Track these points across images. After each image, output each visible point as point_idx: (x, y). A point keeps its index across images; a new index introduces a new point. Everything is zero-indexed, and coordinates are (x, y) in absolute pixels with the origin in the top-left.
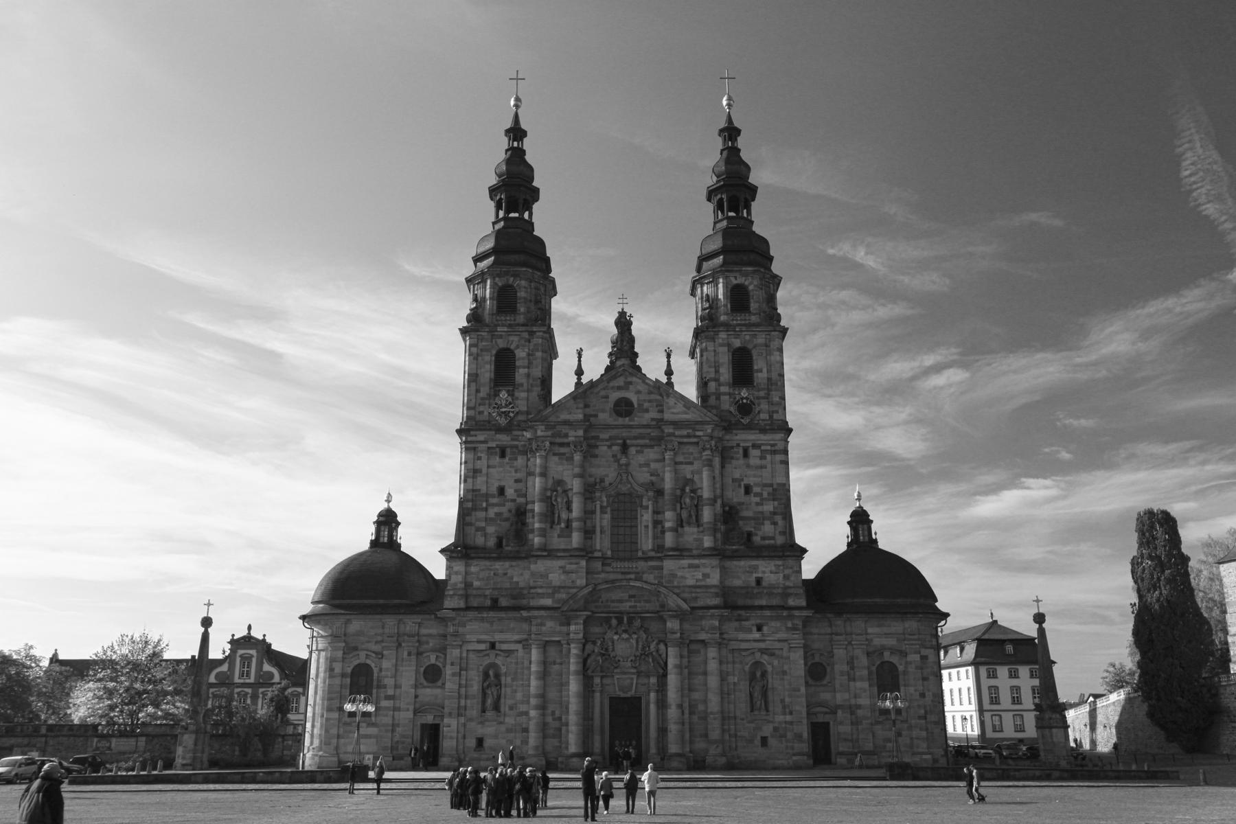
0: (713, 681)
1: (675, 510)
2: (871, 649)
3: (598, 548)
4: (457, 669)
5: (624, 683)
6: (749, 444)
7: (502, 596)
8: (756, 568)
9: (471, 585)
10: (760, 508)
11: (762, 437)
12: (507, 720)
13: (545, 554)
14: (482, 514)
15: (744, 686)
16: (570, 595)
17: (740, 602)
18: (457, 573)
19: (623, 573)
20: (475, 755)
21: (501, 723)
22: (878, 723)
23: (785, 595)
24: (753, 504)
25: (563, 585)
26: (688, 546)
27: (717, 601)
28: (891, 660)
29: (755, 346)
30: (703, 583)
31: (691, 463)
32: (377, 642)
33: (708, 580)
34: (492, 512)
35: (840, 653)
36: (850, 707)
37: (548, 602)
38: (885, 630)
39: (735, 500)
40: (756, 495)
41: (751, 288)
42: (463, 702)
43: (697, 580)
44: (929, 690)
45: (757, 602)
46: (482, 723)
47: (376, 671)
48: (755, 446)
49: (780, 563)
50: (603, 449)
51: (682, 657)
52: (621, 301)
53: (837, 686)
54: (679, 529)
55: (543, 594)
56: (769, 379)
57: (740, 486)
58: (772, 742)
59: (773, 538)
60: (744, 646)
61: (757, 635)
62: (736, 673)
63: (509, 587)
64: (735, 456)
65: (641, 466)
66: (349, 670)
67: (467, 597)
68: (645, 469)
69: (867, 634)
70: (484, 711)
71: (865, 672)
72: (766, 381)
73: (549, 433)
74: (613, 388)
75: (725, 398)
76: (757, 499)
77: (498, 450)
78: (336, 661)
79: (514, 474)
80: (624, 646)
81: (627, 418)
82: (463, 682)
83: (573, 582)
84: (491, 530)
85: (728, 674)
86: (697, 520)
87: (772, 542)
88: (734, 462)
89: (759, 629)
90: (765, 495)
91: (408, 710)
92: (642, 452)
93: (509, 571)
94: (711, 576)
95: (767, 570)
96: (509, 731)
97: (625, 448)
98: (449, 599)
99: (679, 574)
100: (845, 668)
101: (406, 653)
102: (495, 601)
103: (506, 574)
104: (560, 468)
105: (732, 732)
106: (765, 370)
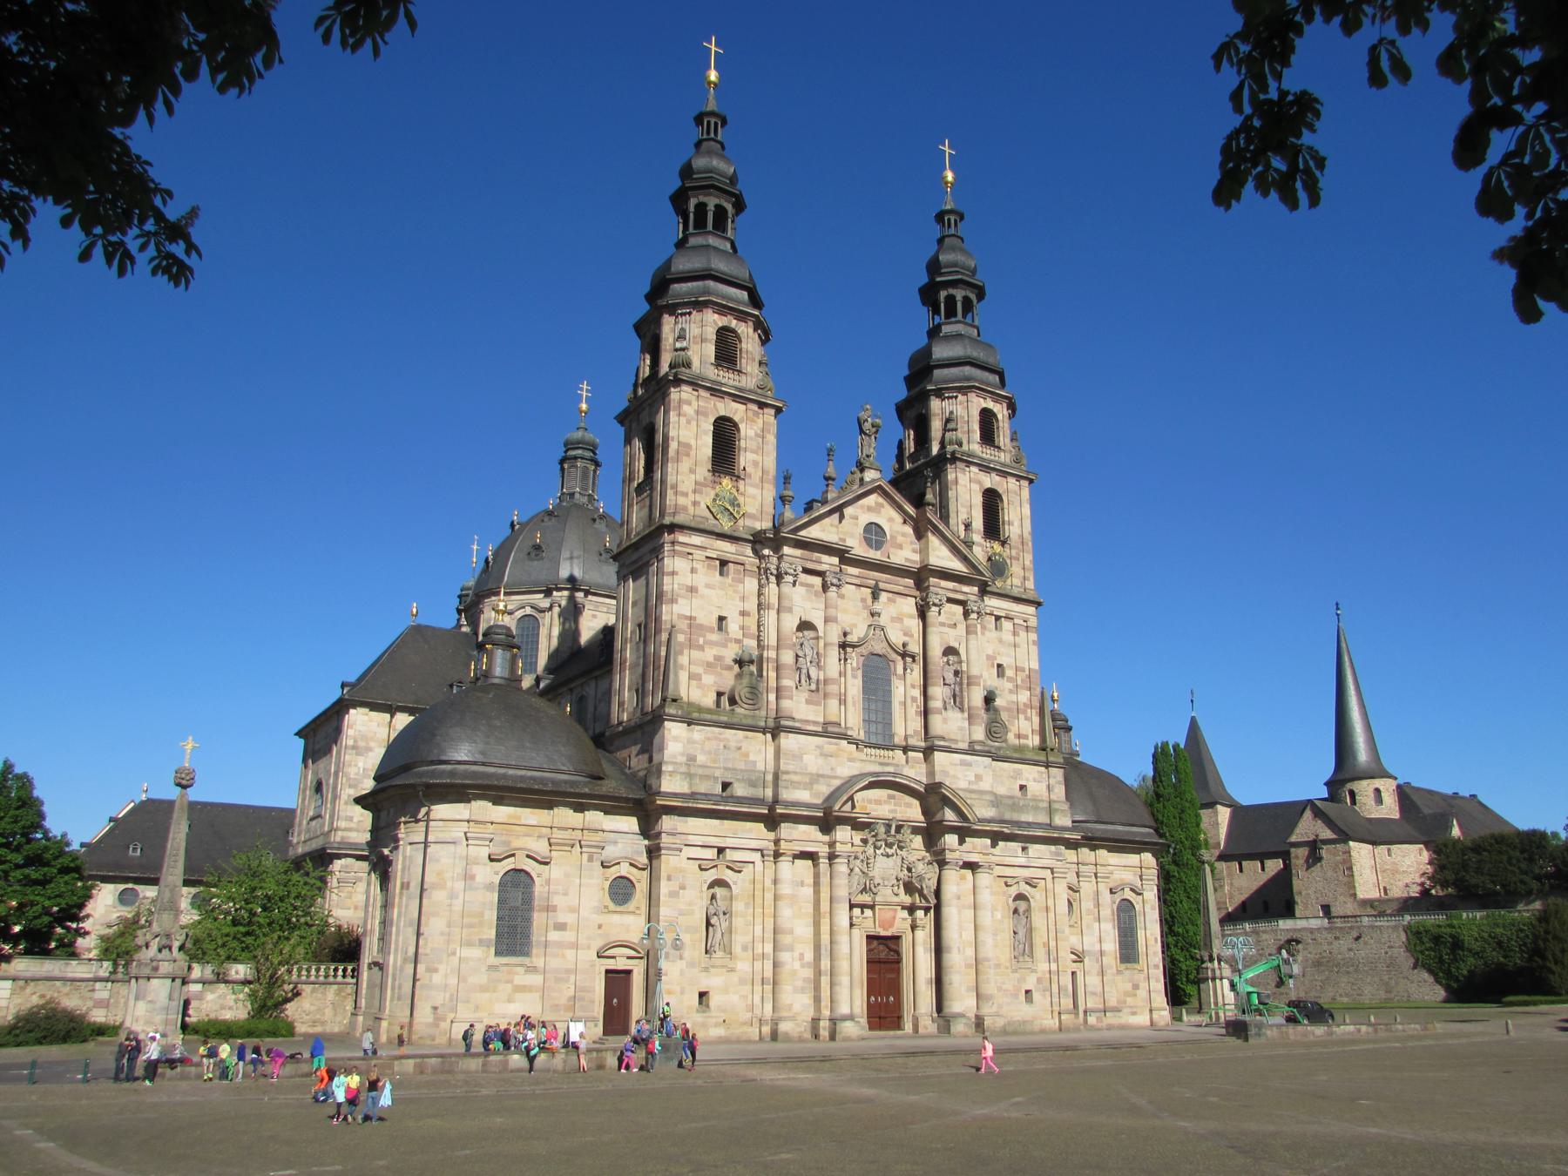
4: (674, 885)
6: (1002, 614)
7: (738, 780)
10: (1014, 698)
14: (695, 654)
16: (832, 789)
18: (676, 739)
19: (881, 764)
20: (699, 1018)
21: (732, 970)
22: (1119, 972)
23: (1051, 811)
24: (1007, 691)
25: (821, 772)
30: (974, 787)
32: (539, 837)
33: (981, 783)
34: (709, 654)
37: (803, 796)
46: (706, 969)
49: (1043, 769)
50: (848, 590)
55: (799, 783)
58: (1036, 996)
59: (1026, 737)
63: (743, 767)
65: (894, 620)
66: (497, 880)
68: (897, 625)
74: (862, 507)
76: (1010, 685)
77: (718, 562)
78: (478, 864)
81: (879, 552)
83: (832, 769)
86: (962, 703)
91: (589, 948)
92: (895, 602)
93: (745, 745)
94: (984, 777)
95: (1031, 778)
96: (742, 982)
98: (668, 778)
99: (951, 772)
101: (585, 856)
103: (740, 748)
104: (808, 605)
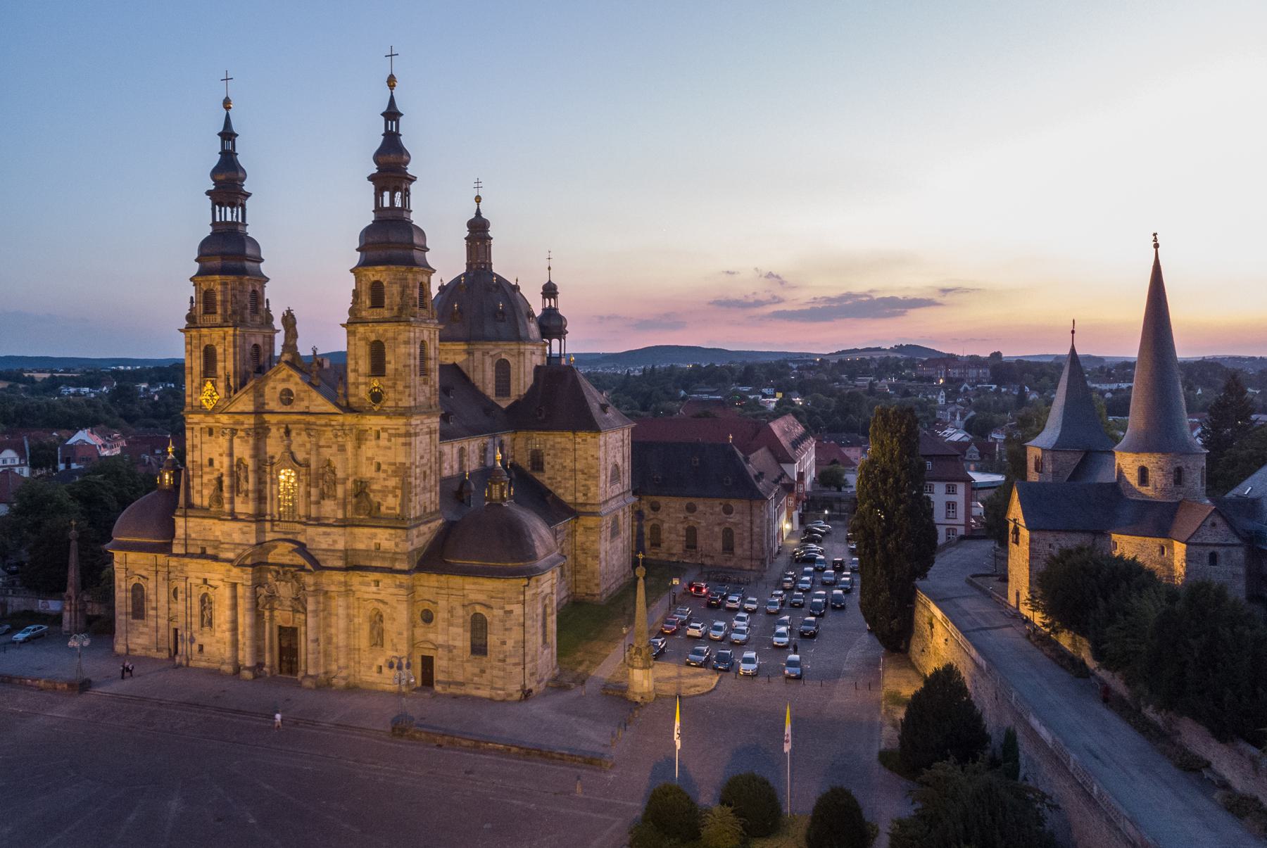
0: (342, 623)
1: (317, 486)
2: (466, 603)
3: (268, 511)
5: (283, 616)
8: (375, 535)
9: (190, 536)
11: (388, 421)
12: (217, 634)
13: (230, 518)
15: (366, 627)
17: (363, 563)
18: (180, 527)
19: (285, 533)
23: (394, 560)
24: (382, 480)
26: (327, 515)
27: (340, 563)
28: (482, 612)
29: (386, 340)
30: (332, 548)
31: (330, 447)
35: (442, 603)
36: (449, 647)
37: (231, 555)
38: (478, 587)
39: (368, 475)
40: (385, 471)
41: (385, 284)
42: (189, 619)
43: (329, 545)
44: (510, 638)
45: (374, 564)
46: (201, 634)
47: (145, 589)
48: (384, 430)
51: (318, 603)
52: (480, 185)
53: (439, 630)
54: (322, 502)
56: (396, 370)
57: (372, 464)
59: (394, 509)
60: (366, 596)
61: (374, 589)
62: (361, 616)
64: (369, 438)
66: (130, 587)
67: (186, 545)
68: (302, 449)
69: (463, 589)
70: (202, 626)
71: (461, 620)
72: (393, 372)
73: (231, 421)
74: (279, 379)
75: (362, 387)
79: (218, 449)
80: (285, 590)
82: (189, 605)
84: (206, 492)
85: (354, 616)
87: (393, 511)
88: (368, 442)
89: (377, 583)
90: (390, 472)
92: (298, 434)
93: (213, 527)
95: (384, 537)
96: (218, 642)
97: (288, 432)
99: (317, 539)
100: (446, 615)
102: (204, 550)
105: (357, 659)
106: (393, 362)
